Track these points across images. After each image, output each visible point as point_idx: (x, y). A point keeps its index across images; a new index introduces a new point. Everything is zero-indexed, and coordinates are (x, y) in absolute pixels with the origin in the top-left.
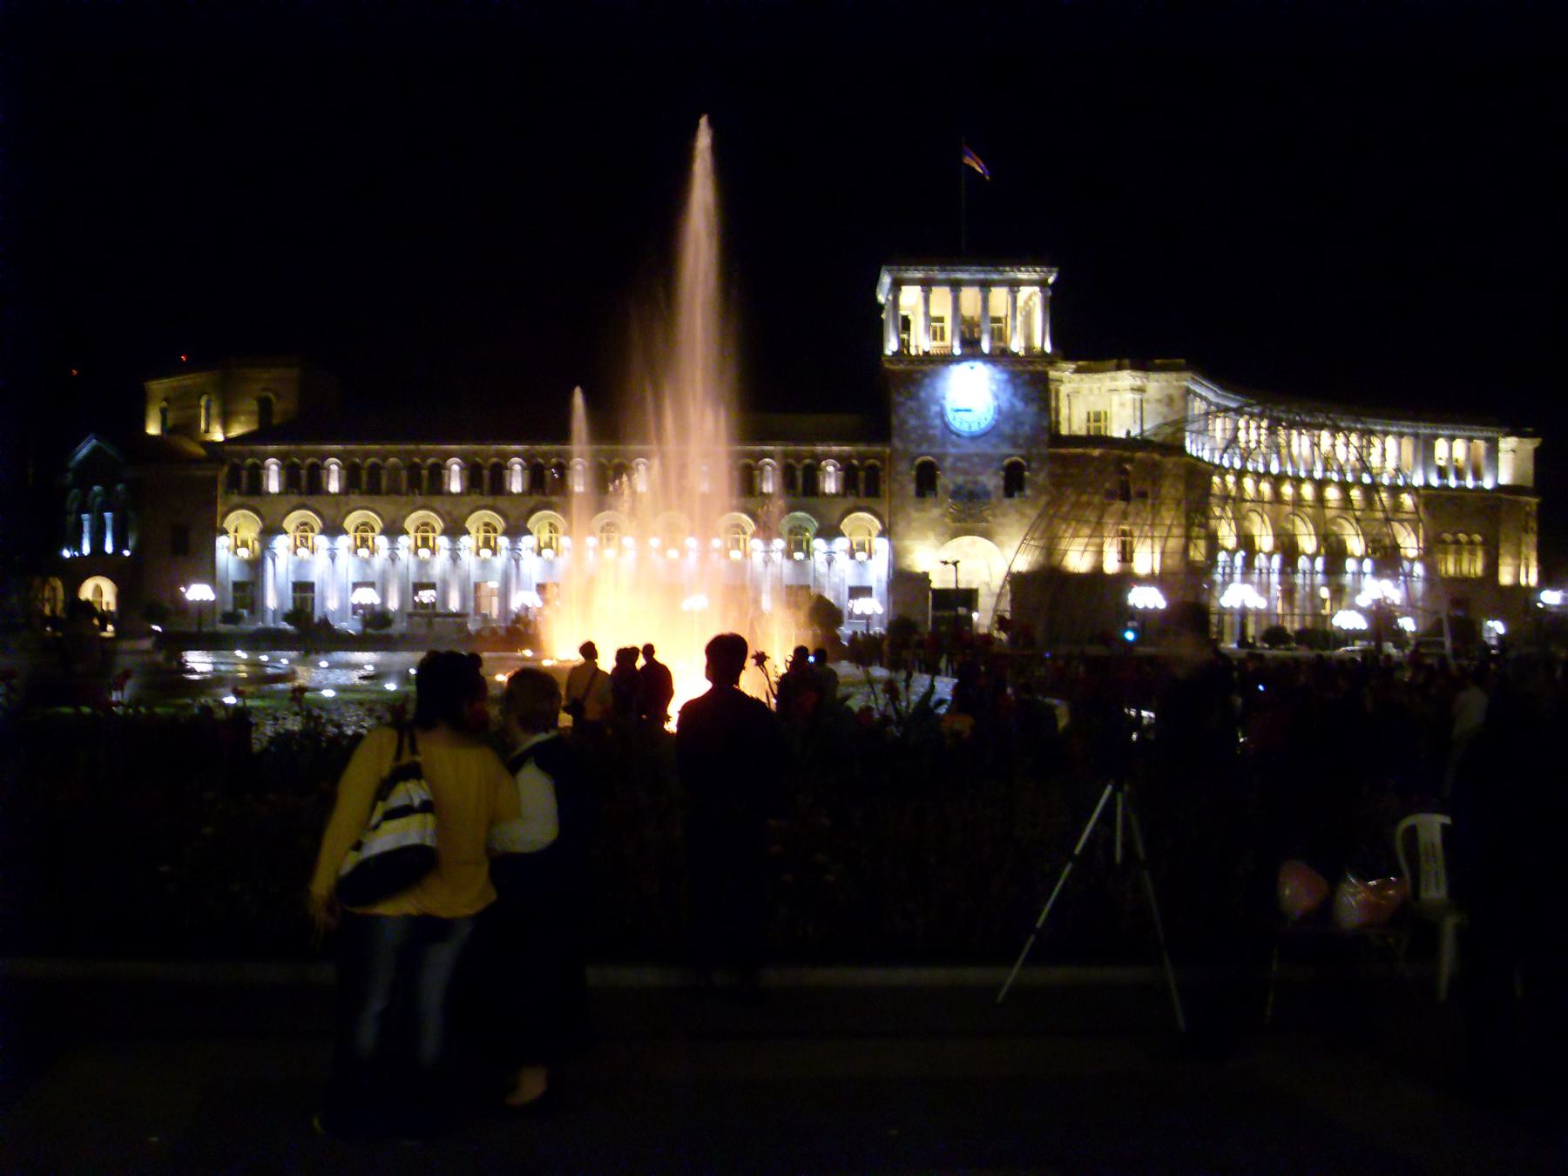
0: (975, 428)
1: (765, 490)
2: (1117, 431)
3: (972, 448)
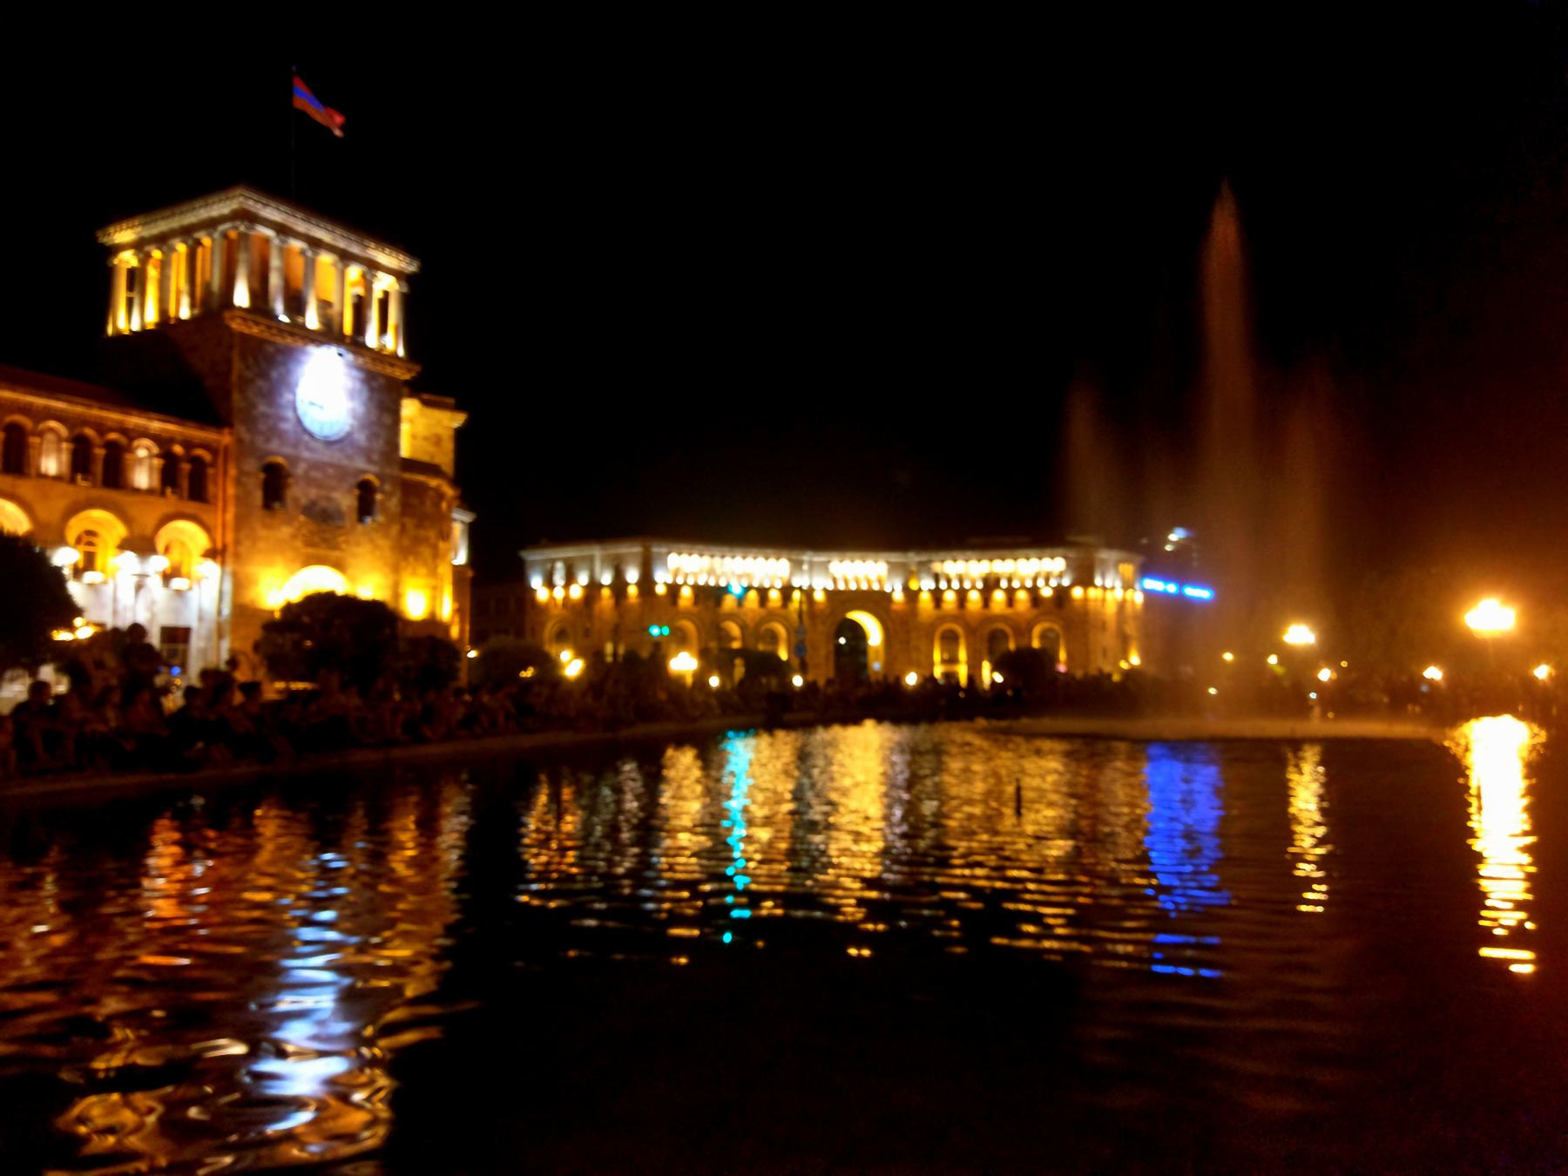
1: (43, 469)
3: (326, 456)
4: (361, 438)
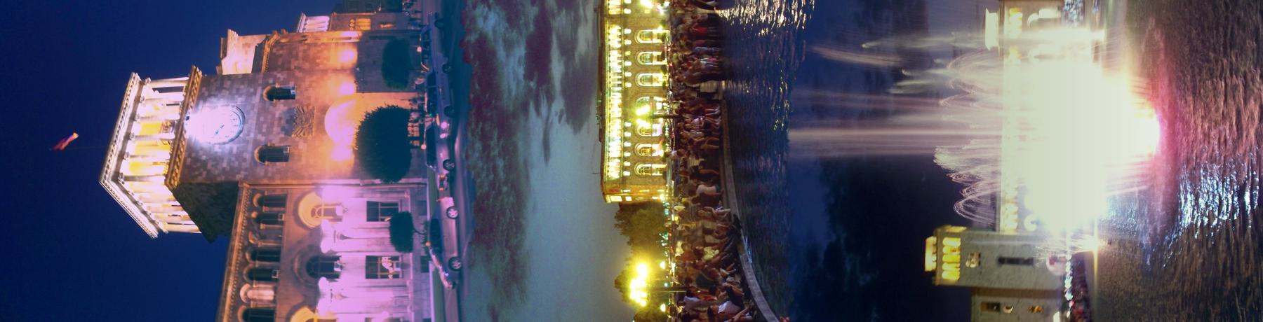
0: (237, 122)
3: (252, 121)
4: (240, 100)
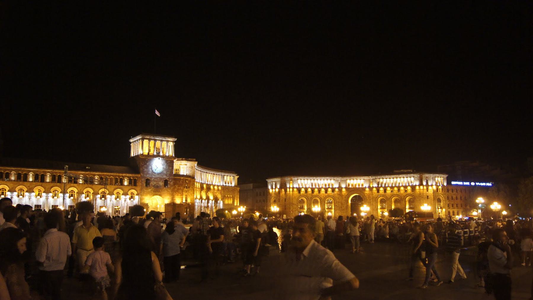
2: (181, 173)
3: (158, 176)
4: (165, 172)
